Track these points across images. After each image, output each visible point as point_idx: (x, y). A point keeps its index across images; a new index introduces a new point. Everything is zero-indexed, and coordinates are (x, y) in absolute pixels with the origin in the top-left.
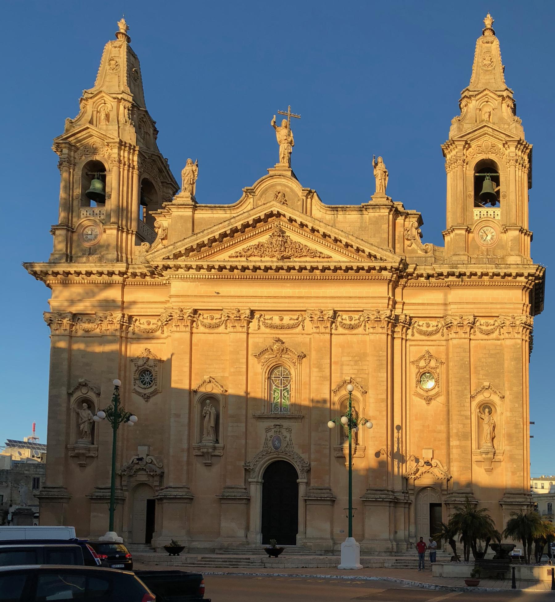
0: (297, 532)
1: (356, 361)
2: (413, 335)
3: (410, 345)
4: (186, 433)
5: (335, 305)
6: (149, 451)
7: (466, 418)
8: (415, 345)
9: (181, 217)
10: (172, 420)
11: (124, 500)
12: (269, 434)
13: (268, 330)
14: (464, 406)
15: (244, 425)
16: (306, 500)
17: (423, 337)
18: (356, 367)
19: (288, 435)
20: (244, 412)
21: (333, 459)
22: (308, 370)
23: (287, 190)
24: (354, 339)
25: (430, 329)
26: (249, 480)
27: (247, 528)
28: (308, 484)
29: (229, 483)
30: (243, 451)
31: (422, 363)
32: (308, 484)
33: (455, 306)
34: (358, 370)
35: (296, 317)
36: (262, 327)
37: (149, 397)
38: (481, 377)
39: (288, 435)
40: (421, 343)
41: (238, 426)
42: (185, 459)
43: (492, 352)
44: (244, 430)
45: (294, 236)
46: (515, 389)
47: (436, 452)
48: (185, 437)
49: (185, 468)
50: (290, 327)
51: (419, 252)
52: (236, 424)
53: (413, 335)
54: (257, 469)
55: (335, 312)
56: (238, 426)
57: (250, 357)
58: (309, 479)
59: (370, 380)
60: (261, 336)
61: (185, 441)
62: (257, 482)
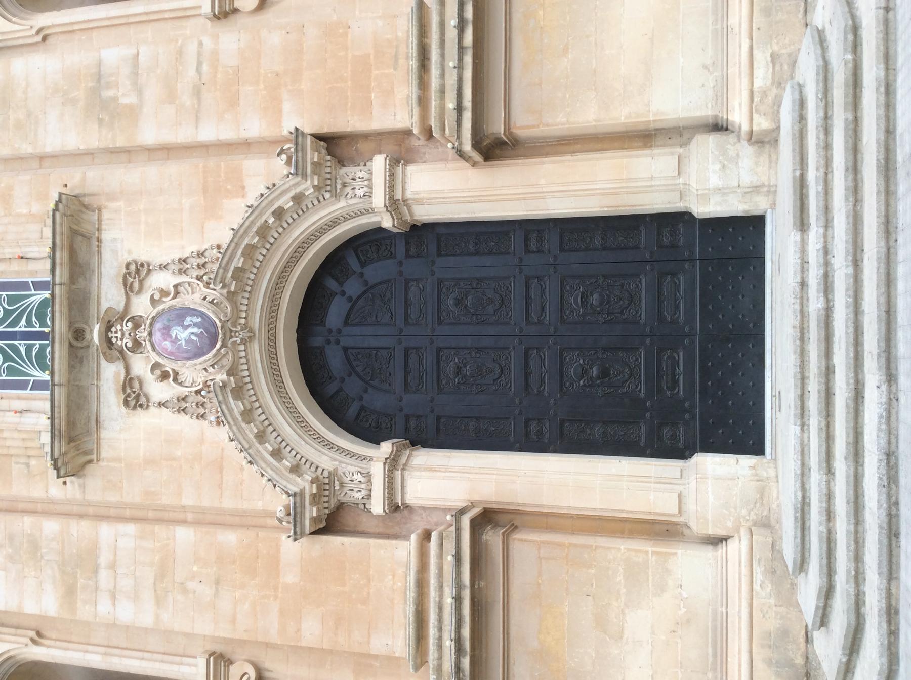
15: (106, 531)
16: (492, 149)
19: (162, 280)
20: (51, 526)
26: (377, 506)
28: (401, 148)
29: (396, 640)
30: (230, 538)
32: (401, 148)
41: (113, 566)
44: (130, 528)
52: (104, 575)
54: (326, 461)
56: (113, 566)
58: (378, 139)
62: (392, 463)
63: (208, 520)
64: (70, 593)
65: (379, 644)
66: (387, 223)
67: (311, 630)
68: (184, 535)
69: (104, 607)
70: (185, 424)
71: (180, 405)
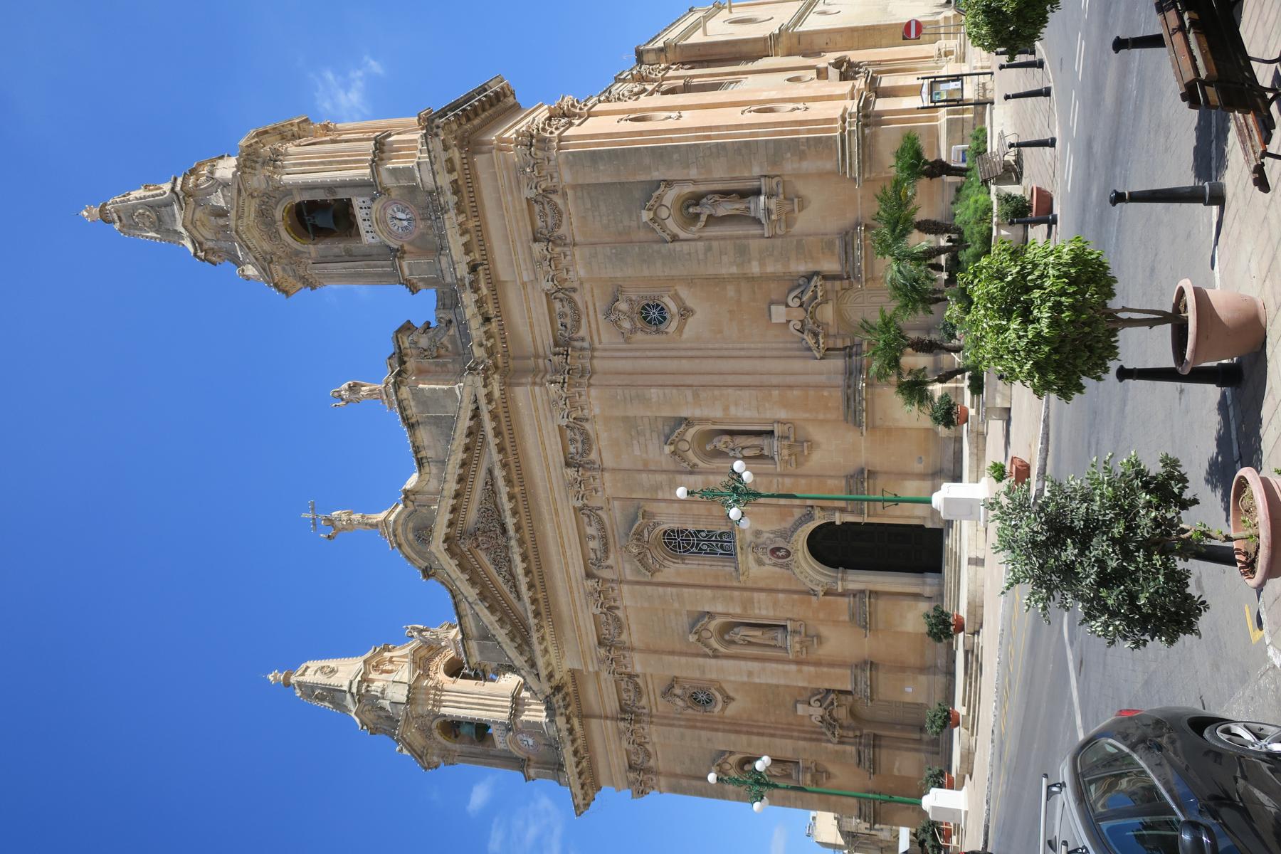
0: (922, 526)
1: (638, 433)
2: (583, 340)
3: (600, 343)
4: (774, 665)
5: (558, 465)
6: (803, 702)
7: (709, 249)
8: (599, 335)
9: (481, 652)
10: (757, 680)
11: (875, 736)
12: (767, 561)
13: (612, 556)
14: (689, 254)
15: (756, 595)
17: (584, 321)
18: (648, 435)
20: (736, 593)
21: (799, 471)
22: (662, 505)
23: (411, 525)
24: (604, 436)
25: (567, 310)
27: (917, 596)
30: (796, 596)
31: (626, 325)
33: (524, 273)
34: (652, 431)
35: (586, 519)
36: (610, 562)
37: (728, 697)
38: (634, 224)
39: (766, 535)
40: (594, 326)
42: (812, 669)
43: (589, 206)
45: (472, 515)
46: (647, 161)
47: (774, 297)
48: (780, 667)
49: (825, 670)
50: (602, 528)
51: (451, 332)
53: (583, 340)
55: (568, 465)
57: (655, 580)
59: (664, 414)
60: (621, 565)
61: (786, 667)
63: (783, 591)
64: (745, 608)
65: (841, 618)
66: (838, 523)
67: (821, 615)
68: (781, 596)
69: (757, 611)
70: (777, 569)
71: (775, 565)
